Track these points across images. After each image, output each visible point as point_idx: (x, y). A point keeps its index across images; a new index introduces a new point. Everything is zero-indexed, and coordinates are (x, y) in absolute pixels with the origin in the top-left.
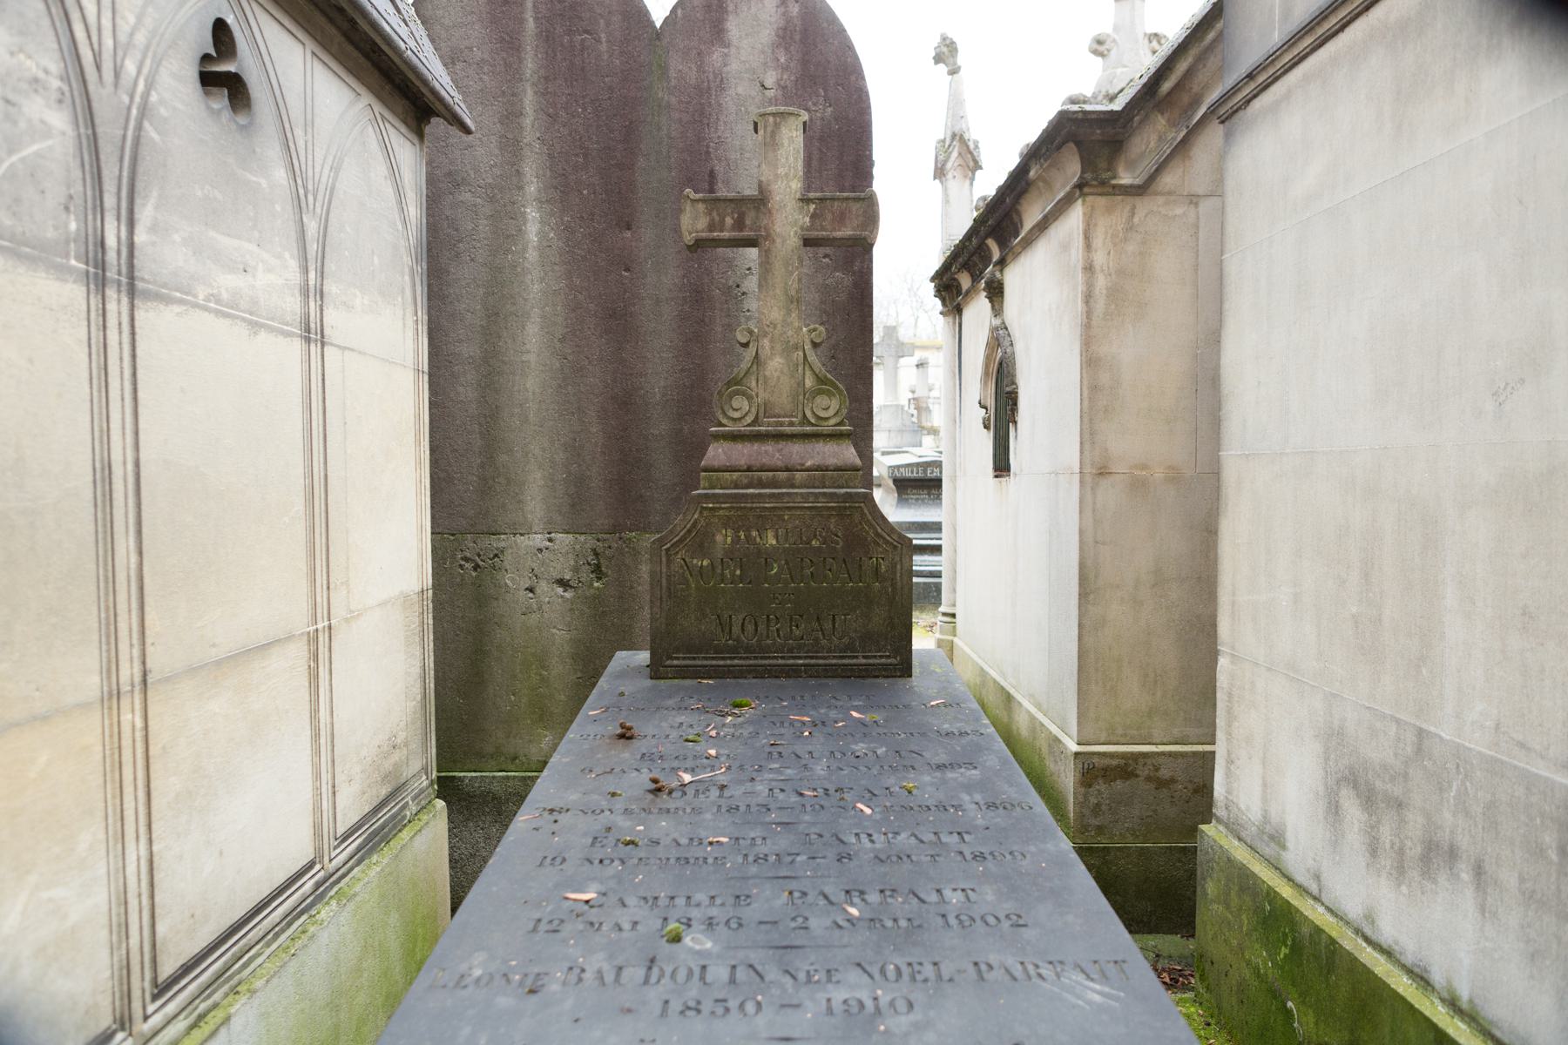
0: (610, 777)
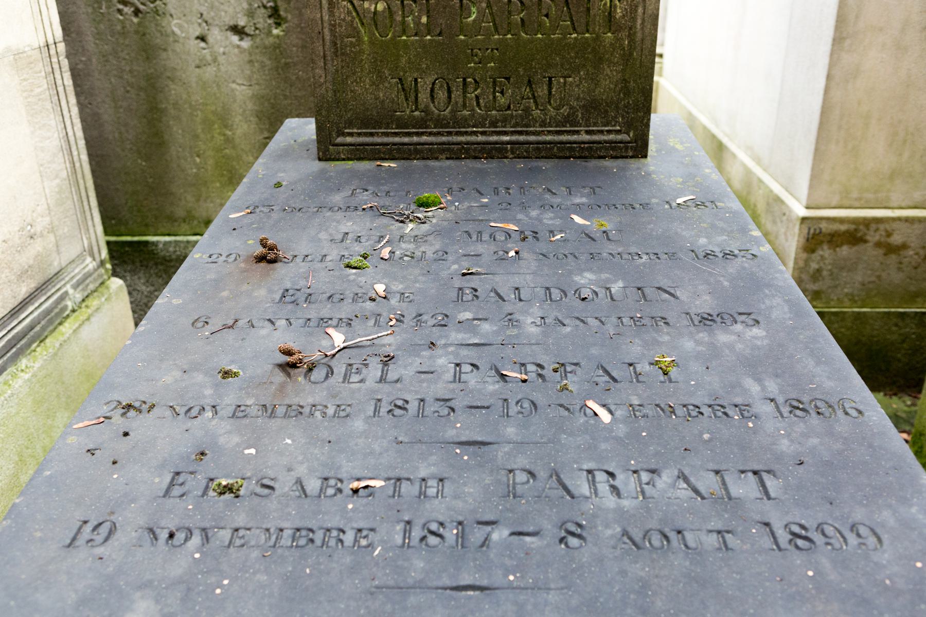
0: (230, 335)
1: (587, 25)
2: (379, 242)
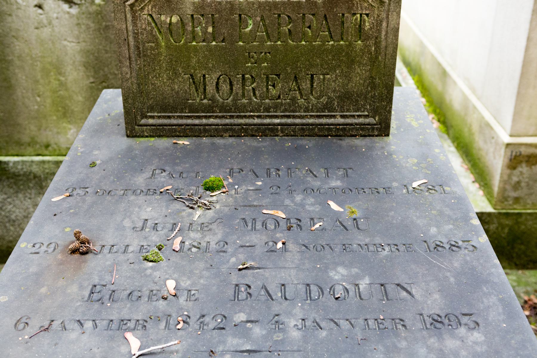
0: (46, 339)
1: (342, 34)
2: (172, 230)
